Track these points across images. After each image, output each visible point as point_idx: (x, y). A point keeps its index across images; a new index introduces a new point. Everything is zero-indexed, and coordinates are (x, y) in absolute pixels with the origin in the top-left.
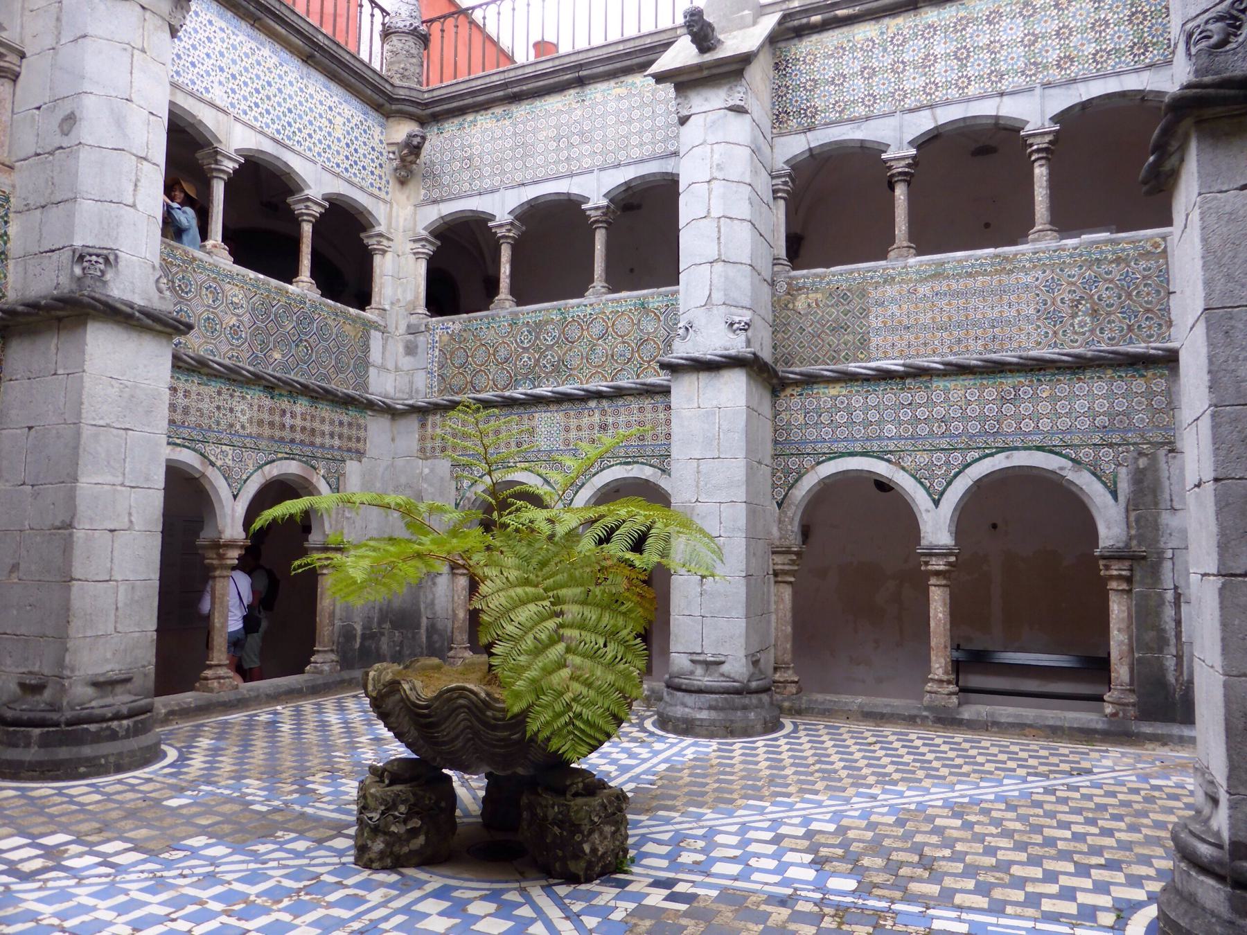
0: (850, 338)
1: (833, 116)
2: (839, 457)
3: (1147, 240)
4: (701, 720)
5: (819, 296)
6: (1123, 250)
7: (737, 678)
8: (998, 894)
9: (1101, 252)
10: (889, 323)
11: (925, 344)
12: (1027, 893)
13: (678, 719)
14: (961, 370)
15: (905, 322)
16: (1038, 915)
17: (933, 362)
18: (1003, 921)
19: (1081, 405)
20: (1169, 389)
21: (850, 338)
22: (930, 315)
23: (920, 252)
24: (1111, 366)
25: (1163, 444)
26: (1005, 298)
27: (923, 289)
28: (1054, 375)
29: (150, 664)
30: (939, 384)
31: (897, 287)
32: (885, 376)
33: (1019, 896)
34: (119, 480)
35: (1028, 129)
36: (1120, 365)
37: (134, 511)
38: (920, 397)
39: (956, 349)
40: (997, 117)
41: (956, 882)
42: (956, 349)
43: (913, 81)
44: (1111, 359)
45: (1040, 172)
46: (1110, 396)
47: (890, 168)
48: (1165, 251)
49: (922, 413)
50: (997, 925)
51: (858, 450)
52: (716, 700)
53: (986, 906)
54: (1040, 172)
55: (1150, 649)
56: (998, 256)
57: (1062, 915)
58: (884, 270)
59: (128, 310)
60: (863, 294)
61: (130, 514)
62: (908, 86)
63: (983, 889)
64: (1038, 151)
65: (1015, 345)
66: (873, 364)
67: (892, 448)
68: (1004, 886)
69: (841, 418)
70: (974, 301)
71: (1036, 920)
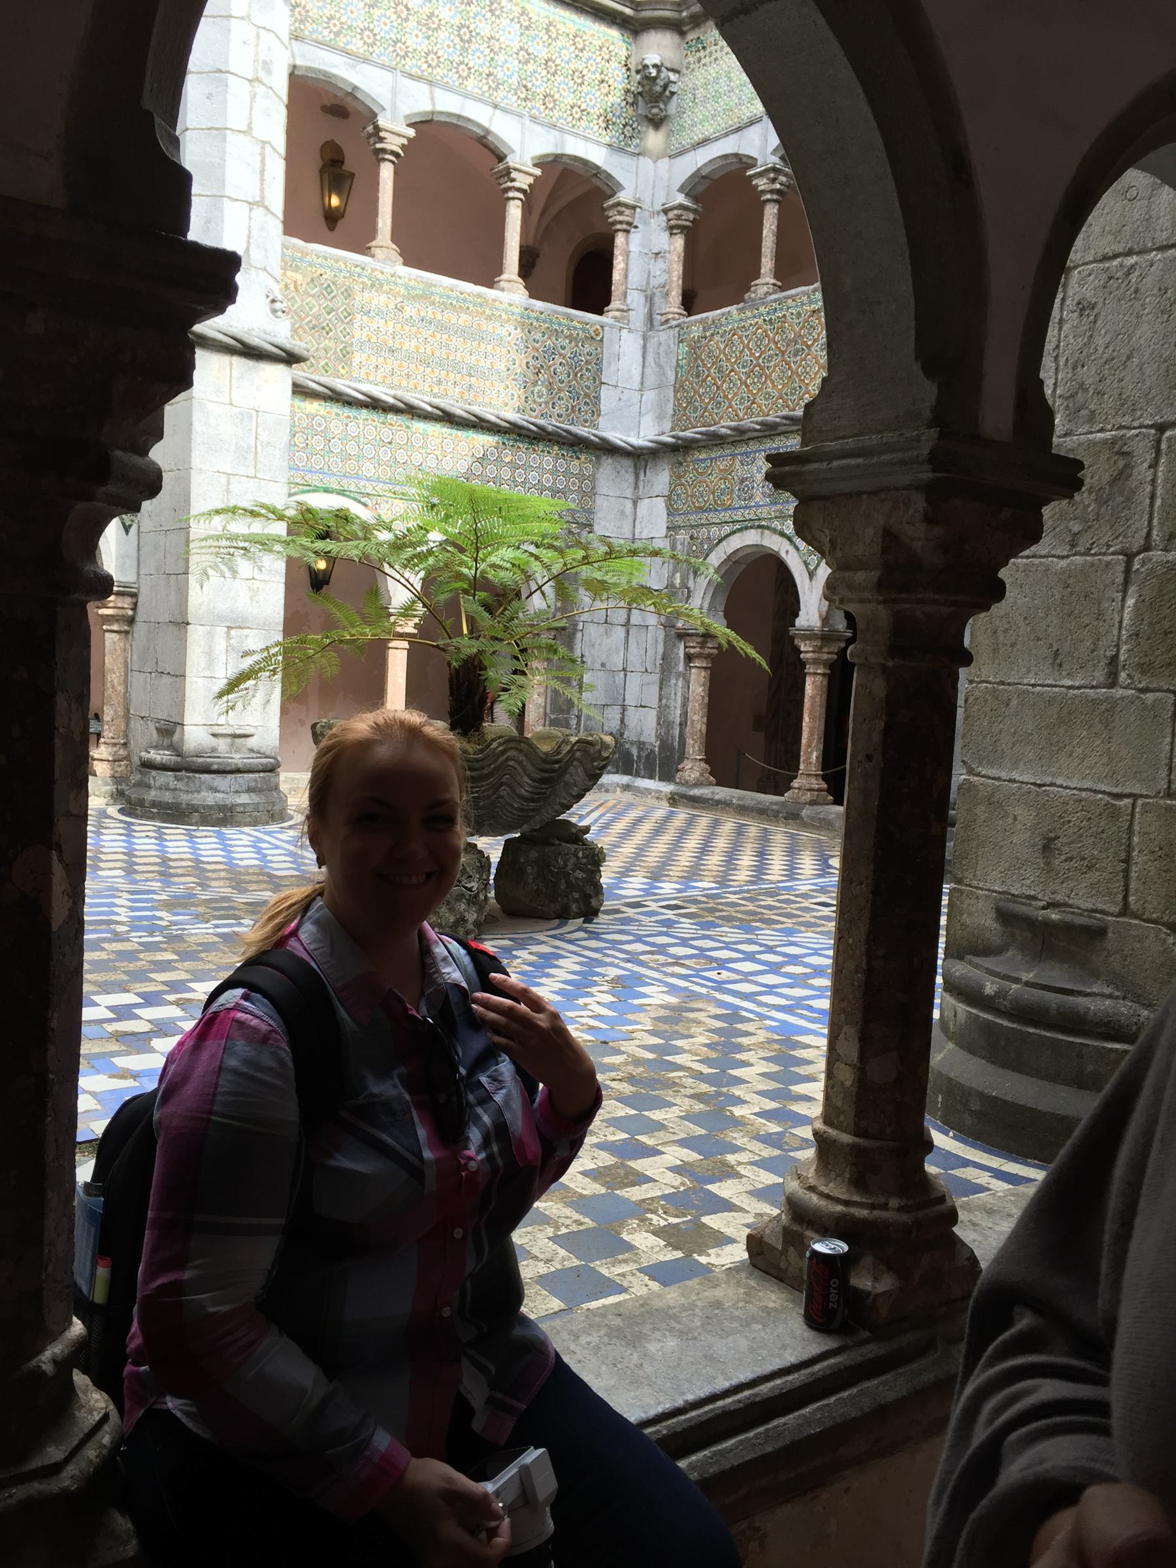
0: (331, 344)
1: (327, 35)
2: (314, 491)
3: (593, 325)
4: (244, 805)
5: (299, 277)
6: (575, 328)
7: (268, 753)
9: (560, 324)
10: (374, 340)
11: (408, 376)
13: (210, 807)
14: (447, 418)
15: (390, 343)
17: (421, 400)
19: (533, 477)
20: (593, 475)
21: (331, 344)
22: (414, 343)
23: (405, 264)
24: (558, 442)
25: (586, 525)
26: (483, 346)
27: (410, 310)
28: (516, 441)
30: (419, 426)
31: (383, 298)
32: (374, 404)
35: (512, 161)
36: (564, 444)
38: (400, 437)
39: (436, 390)
40: (488, 132)
42: (436, 390)
43: (415, 41)
44: (564, 437)
45: (514, 212)
46: (554, 472)
47: (381, 140)
48: (602, 340)
49: (401, 455)
51: (334, 486)
52: (256, 781)
54: (514, 212)
55: (562, 711)
56: (479, 295)
58: (373, 270)
60: (348, 294)
62: (412, 42)
64: (519, 190)
65: (487, 400)
66: (365, 388)
67: (369, 490)
69: (317, 443)
70: (456, 341)
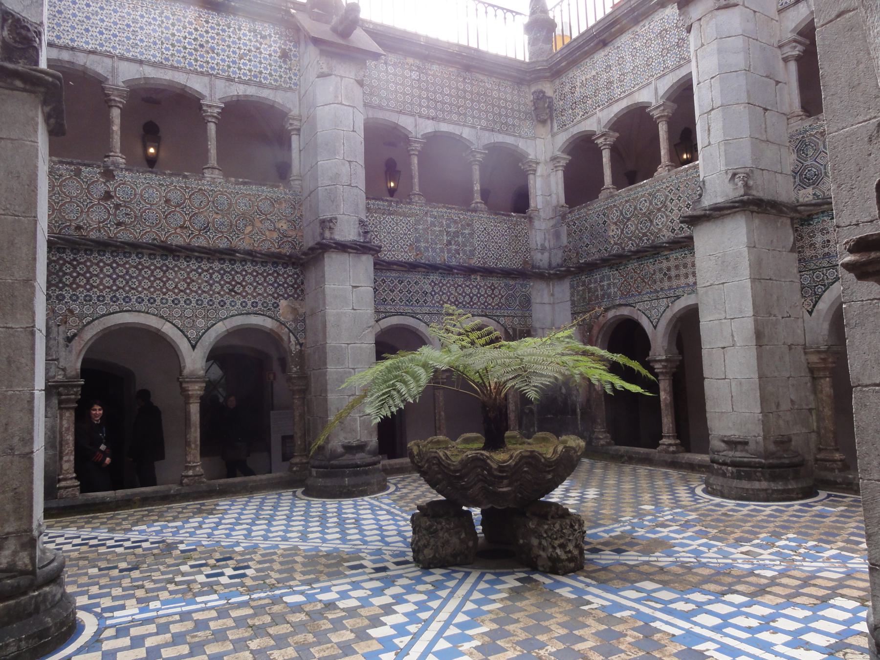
8: (189, 625)
12: (169, 632)
16: (157, 621)
18: (179, 610)
29: (759, 435)
33: (175, 628)
34: (723, 316)
37: (735, 334)
41: (224, 624)
50: (181, 607)
53: (193, 615)
57: (141, 625)
59: (703, 213)
61: (733, 336)
63: (201, 625)
68: (188, 632)
71: (158, 617)
